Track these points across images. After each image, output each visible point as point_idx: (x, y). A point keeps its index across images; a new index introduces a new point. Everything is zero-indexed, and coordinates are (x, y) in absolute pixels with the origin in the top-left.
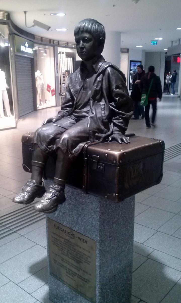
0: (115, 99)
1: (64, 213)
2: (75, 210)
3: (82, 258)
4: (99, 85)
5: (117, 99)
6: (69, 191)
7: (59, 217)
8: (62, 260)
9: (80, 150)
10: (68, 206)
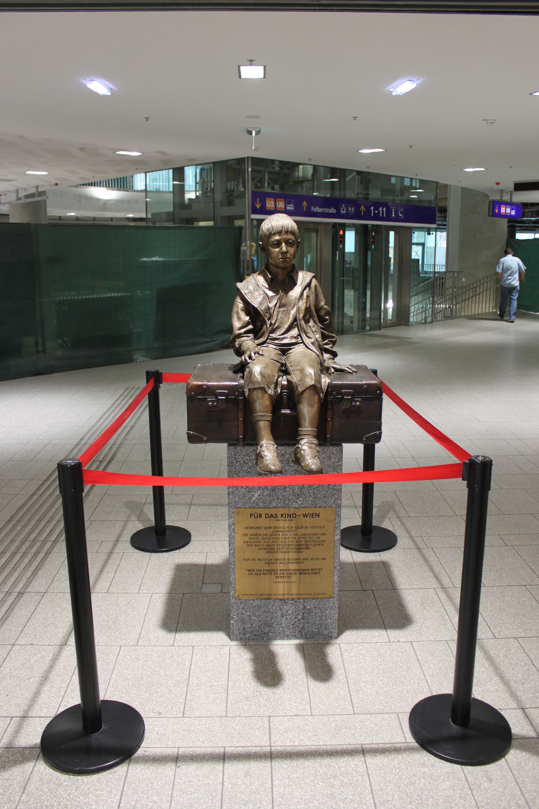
0: (325, 318)
5: (327, 317)
6: (286, 453)
8: (266, 563)
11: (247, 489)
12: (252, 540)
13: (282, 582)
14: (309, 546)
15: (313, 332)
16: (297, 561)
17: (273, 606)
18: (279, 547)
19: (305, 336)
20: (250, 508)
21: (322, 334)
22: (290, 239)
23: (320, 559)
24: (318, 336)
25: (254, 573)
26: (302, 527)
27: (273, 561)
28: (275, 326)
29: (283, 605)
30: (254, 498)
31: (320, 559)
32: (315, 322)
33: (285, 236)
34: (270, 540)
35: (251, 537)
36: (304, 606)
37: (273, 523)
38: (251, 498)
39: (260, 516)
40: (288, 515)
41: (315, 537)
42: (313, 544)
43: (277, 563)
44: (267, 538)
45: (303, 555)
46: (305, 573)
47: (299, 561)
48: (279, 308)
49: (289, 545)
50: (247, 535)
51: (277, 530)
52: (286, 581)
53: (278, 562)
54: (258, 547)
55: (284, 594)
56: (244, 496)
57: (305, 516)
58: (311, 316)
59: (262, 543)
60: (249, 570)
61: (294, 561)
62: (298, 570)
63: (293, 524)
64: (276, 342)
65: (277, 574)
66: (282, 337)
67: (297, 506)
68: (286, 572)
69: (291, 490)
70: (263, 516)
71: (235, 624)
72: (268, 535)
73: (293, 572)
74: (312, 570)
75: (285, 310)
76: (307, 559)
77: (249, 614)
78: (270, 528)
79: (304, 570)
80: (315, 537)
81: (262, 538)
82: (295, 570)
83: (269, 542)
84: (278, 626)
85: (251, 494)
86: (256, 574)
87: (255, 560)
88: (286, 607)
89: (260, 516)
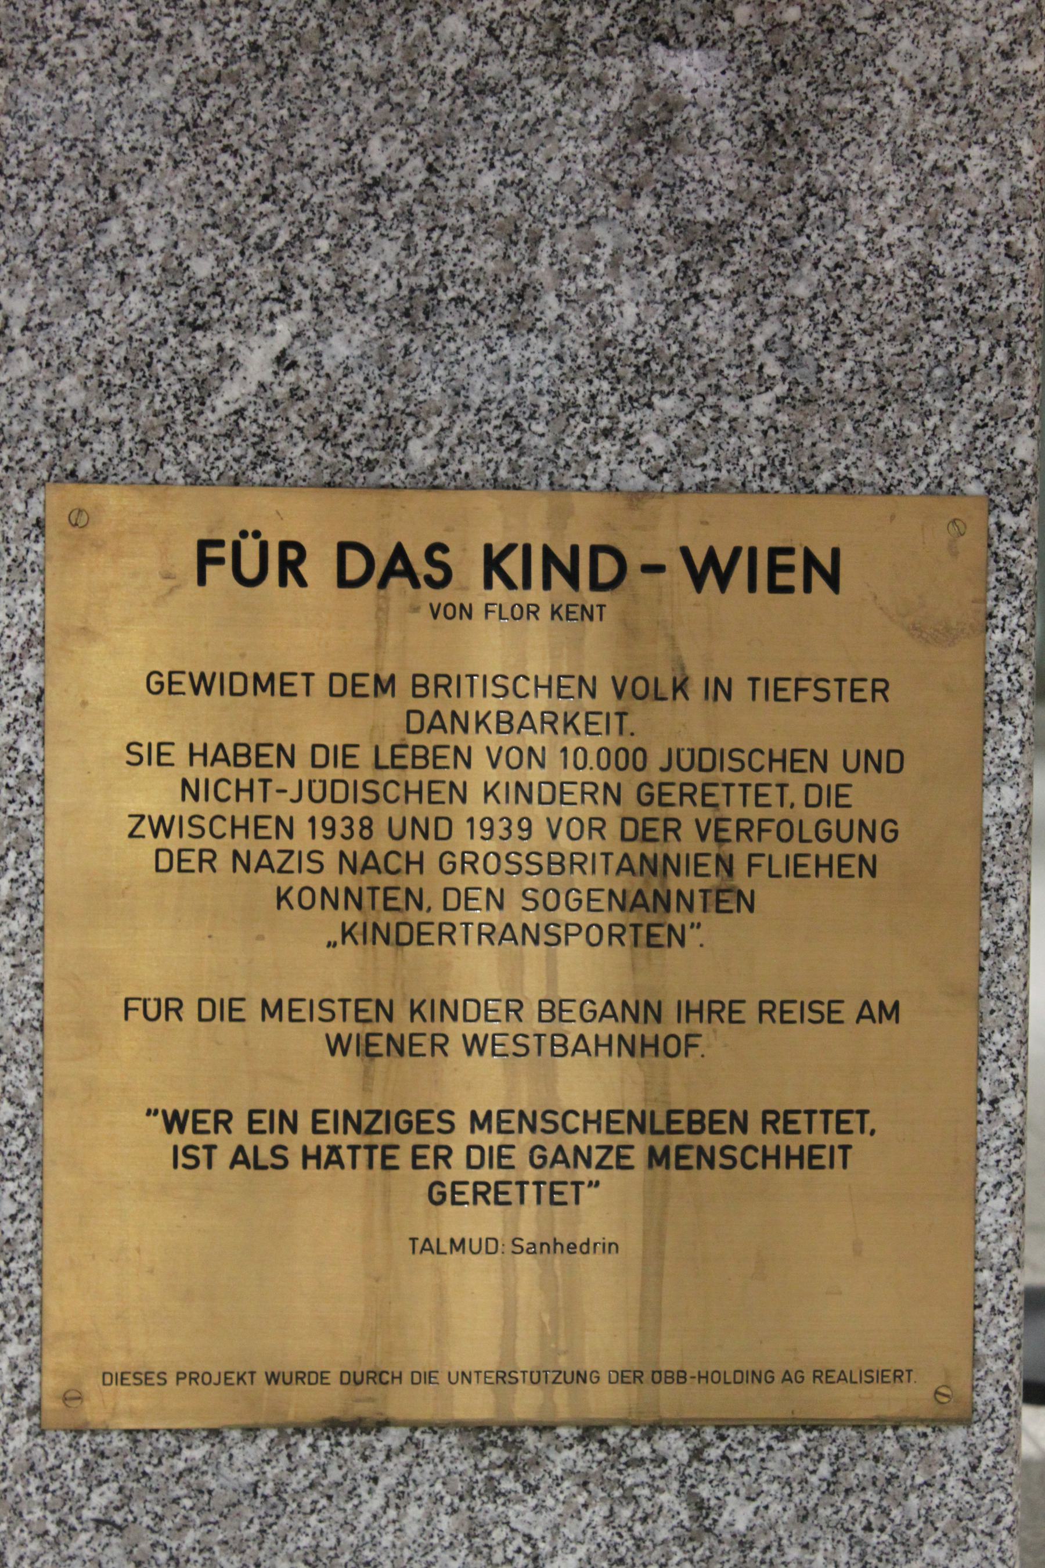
2: (636, 192)
7: (295, 394)
8: (337, 1045)
10: (487, 181)
12: (207, 808)
13: (488, 1246)
14: (742, 881)
16: (629, 1028)
17: (399, 1497)
18: (460, 881)
20: (193, 479)
23: (849, 1011)
25: (225, 1144)
26: (680, 687)
27: (403, 1025)
29: (494, 1492)
30: (233, 392)
31: (849, 1011)
34: (381, 813)
35: (198, 772)
36: (700, 1506)
37: (416, 639)
38: (203, 388)
39: (291, 563)
40: (548, 555)
41: (795, 794)
42: (780, 852)
43: (439, 1045)
44: (352, 792)
45: (683, 974)
46: (706, 1157)
47: (650, 1030)
49: (559, 864)
50: (158, 755)
51: (445, 705)
52: (528, 1233)
53: (455, 1030)
55: (504, 1377)
56: (141, 369)
57: (708, 570)
59: (302, 842)
60: (174, 1121)
61: (608, 1028)
62: (640, 1122)
63: (597, 651)
67: (633, 476)
68: (526, 1139)
69: (576, 318)
70: (319, 568)
72: (364, 756)
73: (592, 1139)
74: (769, 1120)
76: (727, 1011)
78: (384, 685)
79: (702, 1121)
80: (795, 794)
81: (304, 791)
82: (603, 1121)
83: (367, 826)
85: (206, 342)
86: (239, 1158)
87: (229, 1010)
88: (522, 1515)
89: (291, 563)
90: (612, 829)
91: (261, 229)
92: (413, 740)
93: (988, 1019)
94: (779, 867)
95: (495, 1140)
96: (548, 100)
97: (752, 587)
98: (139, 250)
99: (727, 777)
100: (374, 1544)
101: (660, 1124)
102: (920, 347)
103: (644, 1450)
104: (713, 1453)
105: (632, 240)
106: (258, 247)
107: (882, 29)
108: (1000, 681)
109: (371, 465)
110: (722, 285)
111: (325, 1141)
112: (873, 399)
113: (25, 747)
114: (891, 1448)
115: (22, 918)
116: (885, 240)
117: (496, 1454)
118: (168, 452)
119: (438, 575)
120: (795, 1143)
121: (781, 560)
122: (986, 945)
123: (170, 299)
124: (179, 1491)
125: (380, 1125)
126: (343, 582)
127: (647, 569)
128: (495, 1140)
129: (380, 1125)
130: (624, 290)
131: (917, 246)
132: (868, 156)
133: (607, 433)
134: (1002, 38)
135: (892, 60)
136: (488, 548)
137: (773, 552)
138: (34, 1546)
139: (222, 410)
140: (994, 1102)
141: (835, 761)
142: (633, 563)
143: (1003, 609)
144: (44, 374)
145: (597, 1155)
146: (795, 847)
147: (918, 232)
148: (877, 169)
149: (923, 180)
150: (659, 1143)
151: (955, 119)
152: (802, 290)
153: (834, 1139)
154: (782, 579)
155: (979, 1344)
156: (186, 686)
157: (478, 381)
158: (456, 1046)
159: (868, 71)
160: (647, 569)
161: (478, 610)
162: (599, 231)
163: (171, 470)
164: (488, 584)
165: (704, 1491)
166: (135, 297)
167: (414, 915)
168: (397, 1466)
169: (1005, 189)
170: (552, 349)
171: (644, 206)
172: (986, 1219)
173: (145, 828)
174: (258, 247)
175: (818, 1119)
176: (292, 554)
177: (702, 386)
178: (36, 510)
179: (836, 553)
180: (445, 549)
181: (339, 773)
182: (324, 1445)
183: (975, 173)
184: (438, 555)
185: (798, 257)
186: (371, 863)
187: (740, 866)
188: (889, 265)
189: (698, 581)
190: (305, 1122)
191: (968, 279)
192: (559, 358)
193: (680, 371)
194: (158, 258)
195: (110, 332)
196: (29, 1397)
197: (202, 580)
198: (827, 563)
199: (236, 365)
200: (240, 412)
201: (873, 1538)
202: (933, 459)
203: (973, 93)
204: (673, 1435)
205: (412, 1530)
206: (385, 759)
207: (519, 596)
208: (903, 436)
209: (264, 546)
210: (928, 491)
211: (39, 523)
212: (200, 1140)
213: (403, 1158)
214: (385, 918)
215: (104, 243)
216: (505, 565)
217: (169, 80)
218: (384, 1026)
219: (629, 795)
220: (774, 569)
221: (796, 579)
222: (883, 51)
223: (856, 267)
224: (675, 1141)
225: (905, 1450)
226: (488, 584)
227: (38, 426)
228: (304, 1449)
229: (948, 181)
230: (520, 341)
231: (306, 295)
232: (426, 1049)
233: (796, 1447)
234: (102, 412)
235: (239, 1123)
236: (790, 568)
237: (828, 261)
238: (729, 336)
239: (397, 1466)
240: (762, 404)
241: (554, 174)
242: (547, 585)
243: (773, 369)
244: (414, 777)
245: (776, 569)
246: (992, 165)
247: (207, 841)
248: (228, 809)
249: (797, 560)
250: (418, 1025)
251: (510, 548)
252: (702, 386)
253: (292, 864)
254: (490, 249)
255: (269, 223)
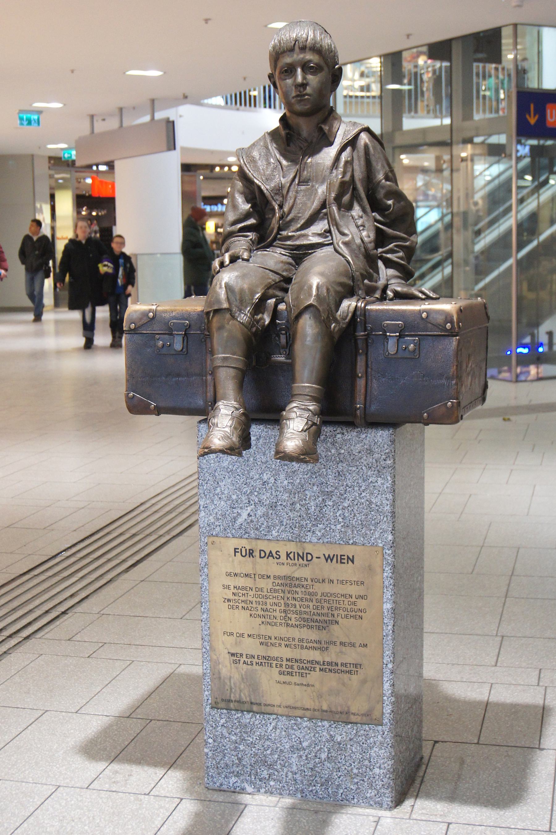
0: (386, 204)
1: (273, 506)
2: (314, 485)
3: (336, 609)
4: (349, 171)
5: (390, 202)
7: (252, 521)
8: (262, 643)
9: (350, 315)
10: (286, 482)
11: (229, 502)
15: (358, 227)
19: (336, 231)
21: (379, 231)
22: (310, 61)
24: (368, 235)
26: (323, 581)
27: (273, 641)
28: (289, 218)
30: (240, 520)
32: (364, 210)
33: (302, 56)
34: (268, 601)
35: (235, 591)
38: (235, 519)
40: (298, 554)
41: (346, 602)
44: (263, 597)
46: (330, 670)
48: (298, 185)
50: (228, 587)
54: (249, 612)
56: (224, 515)
57: (328, 558)
58: (355, 196)
59: (254, 605)
60: (233, 655)
64: (289, 243)
65: (281, 666)
66: (299, 233)
69: (303, 509)
71: (210, 754)
75: (308, 189)
77: (234, 738)
78: (269, 577)
80: (346, 602)
81: (254, 596)
83: (266, 603)
84: (285, 770)
85: (235, 511)
88: (298, 733)
90: (311, 607)
91: (244, 490)
92: (274, 588)
93: (385, 649)
94: (343, 616)
95: (291, 664)
96: (296, 467)
97: (337, 562)
98: (223, 493)
99: (333, 599)
100: (271, 736)
101: (321, 664)
102: (369, 517)
103: (320, 724)
104: (334, 726)
105: (313, 494)
106: (244, 494)
107: (360, 454)
108: (386, 583)
109: (266, 535)
110: (331, 503)
111: (260, 661)
112: (360, 527)
113: (205, 584)
114: (367, 729)
115: (206, 615)
116: (362, 496)
117: (293, 722)
118: (229, 531)
119: (278, 557)
120: (347, 669)
121: (342, 557)
122: (384, 634)
123: (229, 502)
124: (236, 722)
125: (269, 659)
126: (260, 557)
127: (317, 558)
128: (291, 664)
129: (269, 659)
130: (312, 504)
131: (368, 497)
132: (358, 479)
133: (309, 531)
134: (384, 457)
135: (362, 460)
136: (287, 552)
137: (341, 556)
138: (211, 728)
139: (238, 524)
140: (387, 665)
141: (354, 597)
142: (315, 556)
143: (387, 569)
144: (207, 516)
145: (310, 668)
146: (346, 613)
147: (368, 494)
148: (360, 482)
149: (369, 484)
150: (322, 667)
151: (375, 473)
152: (346, 505)
153: (355, 669)
154: (343, 561)
155: (384, 711)
156: (233, 575)
157: (285, 520)
158: (283, 646)
159: (358, 463)
160: (317, 558)
161: (286, 564)
162: (307, 492)
163: (230, 534)
164: (287, 559)
165: (332, 733)
166: (222, 502)
167: (275, 621)
168: (275, 722)
169: (385, 486)
170: (299, 514)
171: (315, 488)
172: (385, 687)
173: (226, 601)
174: (244, 494)
175: (352, 665)
176: (251, 552)
177: (327, 523)
178: (206, 541)
179: (353, 556)
180: (279, 552)
181: (261, 593)
182: (261, 716)
183: (379, 483)
184: (278, 553)
185: (345, 499)
186: (267, 610)
187: (336, 616)
188: (363, 501)
189: (327, 560)
190: (256, 657)
191: (378, 504)
192: (300, 516)
193: (323, 520)
194: (226, 495)
195: (218, 509)
196: (210, 701)
197: (235, 555)
198: (351, 558)
199: (241, 515)
200: (242, 524)
201: (364, 745)
202: (372, 539)
203: (378, 467)
204: (326, 722)
205: (277, 734)
206: (269, 591)
207: (293, 562)
208: (366, 534)
209: (246, 550)
210: (371, 545)
211: (206, 543)
212: (238, 659)
213: (274, 665)
214: (269, 621)
215: (217, 492)
216: (290, 555)
217: (227, 462)
218: (269, 641)
219: (314, 600)
220: (341, 559)
221: (345, 561)
222: (360, 459)
223: (356, 501)
224: (324, 667)
225: (370, 729)
226: (287, 559)
227: (206, 525)
228: (258, 717)
229: (374, 485)
230: (292, 513)
231: (253, 503)
232: (278, 645)
233: (349, 727)
234: (217, 523)
235: (244, 656)
236: (344, 559)
237: (351, 499)
238: (332, 513)
239: (275, 722)
240: (339, 527)
241: (298, 481)
242: (298, 560)
243: (341, 520)
244: (274, 595)
245: (341, 559)
246: (383, 481)
247: (237, 604)
248: (241, 598)
249: (346, 557)
250: (276, 641)
251: (291, 552)
252: (327, 523)
253: (253, 609)
254: (286, 495)
255: (247, 489)
